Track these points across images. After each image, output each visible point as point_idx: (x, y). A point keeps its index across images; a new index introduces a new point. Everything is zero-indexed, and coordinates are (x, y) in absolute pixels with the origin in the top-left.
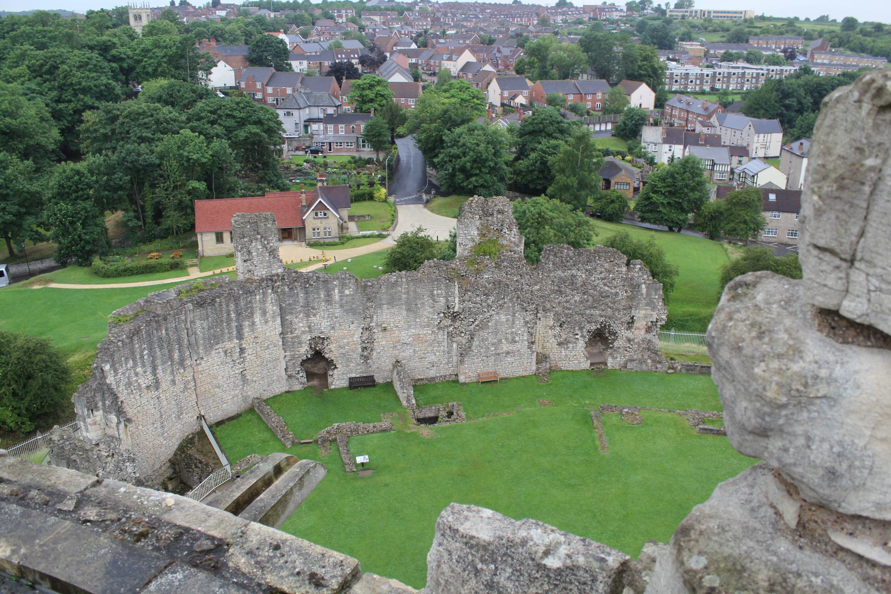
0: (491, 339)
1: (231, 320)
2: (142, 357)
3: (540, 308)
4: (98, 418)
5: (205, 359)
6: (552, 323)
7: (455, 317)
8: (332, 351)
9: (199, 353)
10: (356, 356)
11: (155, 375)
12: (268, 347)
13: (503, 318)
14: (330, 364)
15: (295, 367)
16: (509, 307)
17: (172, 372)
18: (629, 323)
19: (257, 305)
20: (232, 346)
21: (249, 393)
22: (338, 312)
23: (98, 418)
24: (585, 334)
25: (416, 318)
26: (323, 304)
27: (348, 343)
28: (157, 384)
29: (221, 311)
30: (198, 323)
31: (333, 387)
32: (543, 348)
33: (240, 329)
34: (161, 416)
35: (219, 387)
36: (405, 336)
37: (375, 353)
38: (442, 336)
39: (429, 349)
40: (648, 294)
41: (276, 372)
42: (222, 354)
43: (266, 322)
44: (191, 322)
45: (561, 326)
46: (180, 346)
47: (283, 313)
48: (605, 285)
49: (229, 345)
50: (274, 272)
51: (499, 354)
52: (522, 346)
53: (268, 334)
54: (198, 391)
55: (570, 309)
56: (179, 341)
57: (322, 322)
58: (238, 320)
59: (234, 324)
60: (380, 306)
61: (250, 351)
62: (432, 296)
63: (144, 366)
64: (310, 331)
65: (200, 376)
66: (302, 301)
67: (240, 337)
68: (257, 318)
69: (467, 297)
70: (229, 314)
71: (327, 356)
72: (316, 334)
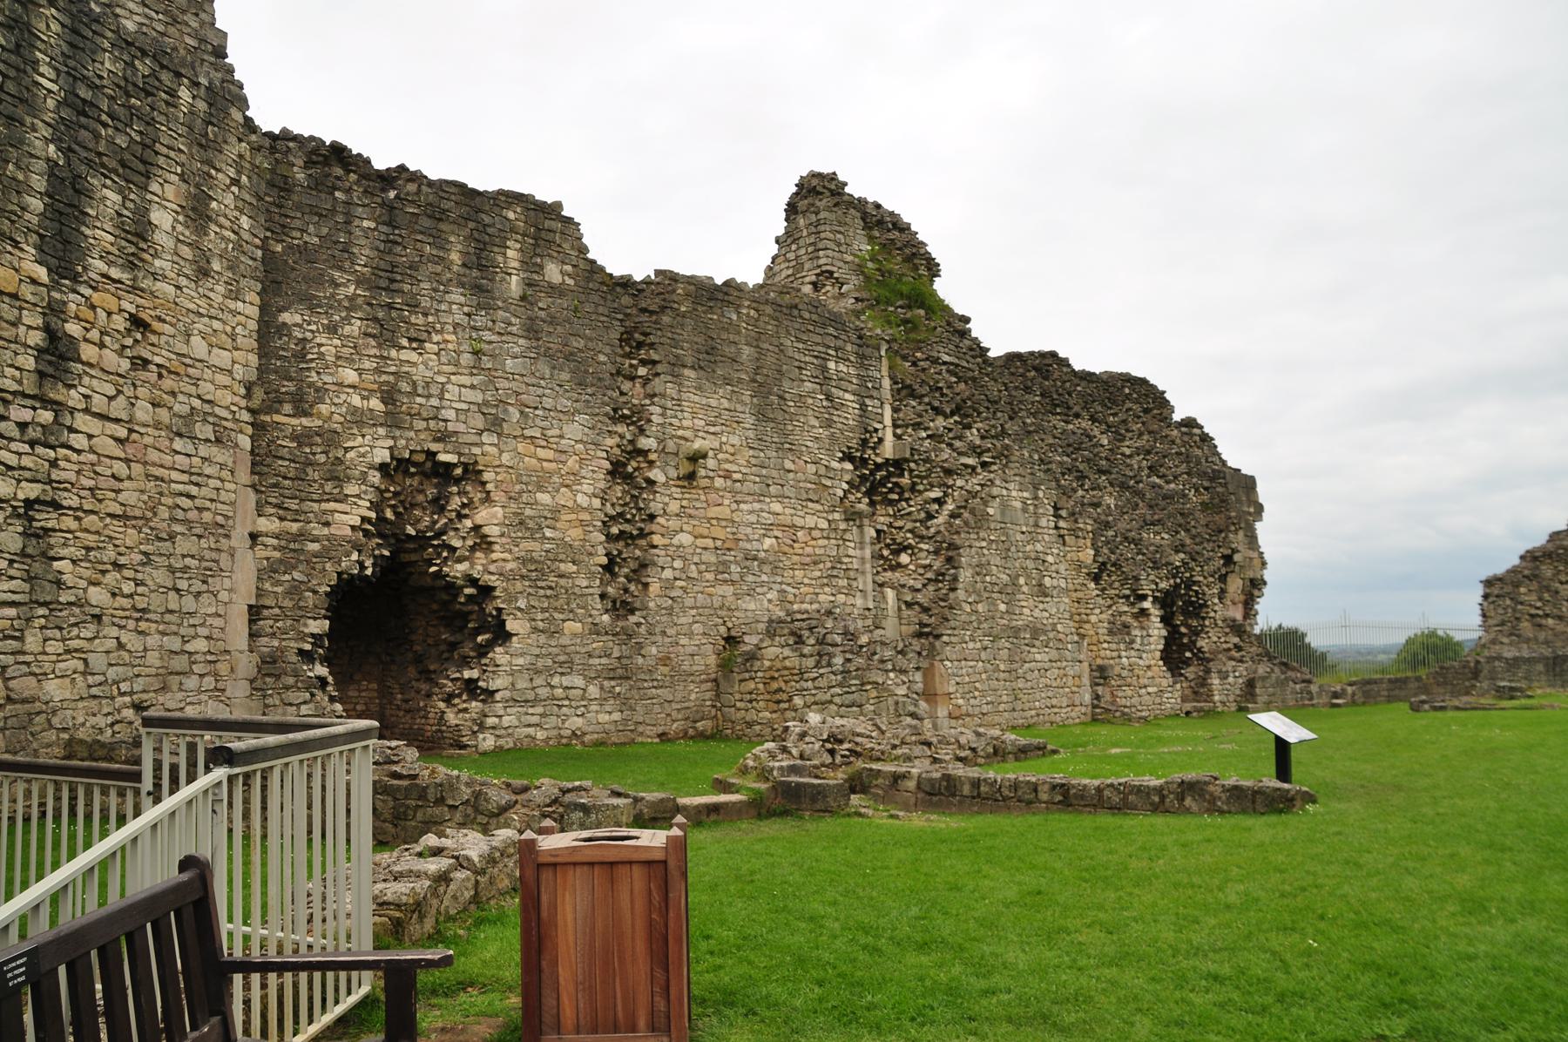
8: (489, 543)
10: (586, 582)
14: (472, 621)
21: (55, 690)
22: (514, 356)
26: (456, 296)
27: (556, 511)
31: (488, 742)
36: (755, 519)
41: (207, 606)
60: (677, 364)
62: (824, 378)
64: (393, 422)
66: (364, 255)
67: (63, 255)
72: (414, 440)
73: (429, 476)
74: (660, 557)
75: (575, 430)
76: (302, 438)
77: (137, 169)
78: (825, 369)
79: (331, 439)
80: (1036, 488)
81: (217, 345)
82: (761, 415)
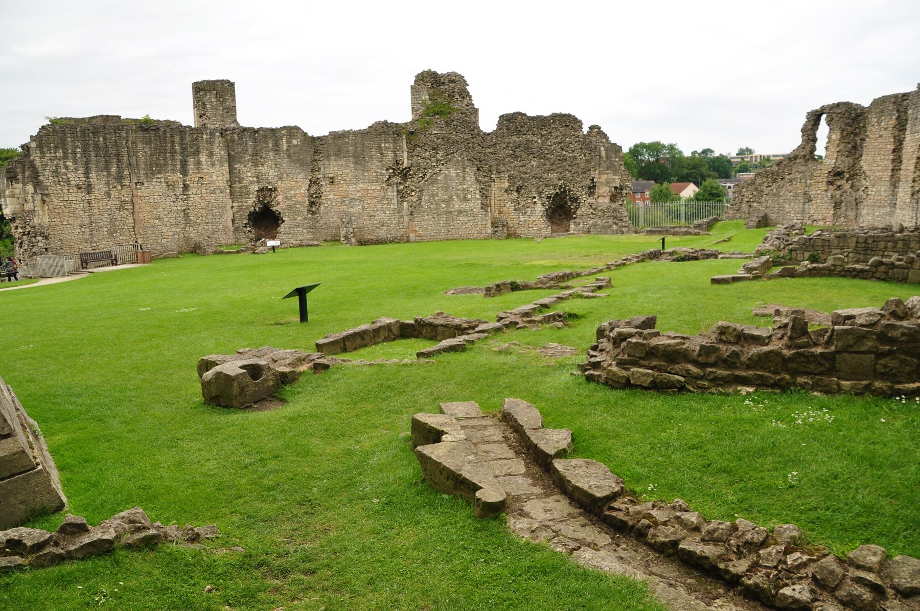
0: (441, 195)
1: (176, 152)
2: (75, 153)
3: (494, 168)
4: (17, 191)
5: (146, 185)
6: (507, 185)
7: (405, 174)
8: (280, 204)
9: (139, 177)
10: (304, 209)
11: (88, 178)
12: (213, 192)
13: (453, 172)
15: (242, 220)
16: (458, 161)
17: (108, 184)
18: (590, 188)
19: (203, 145)
20: (175, 179)
22: (285, 163)
23: (17, 191)
24: (544, 199)
25: (363, 171)
26: (271, 153)
27: (295, 195)
28: (89, 189)
29: (165, 138)
30: (140, 146)
32: (500, 212)
33: (184, 164)
34: (91, 223)
35: (159, 219)
36: (354, 190)
37: (322, 208)
38: (392, 193)
39: (379, 206)
40: (608, 157)
41: (222, 220)
42: (164, 185)
43: (213, 165)
44: (133, 143)
45: (518, 191)
46: (119, 161)
47: (231, 160)
48: (562, 149)
49: (172, 178)
50: (227, 126)
51: (451, 212)
52: (475, 204)
53: (214, 178)
54: (136, 214)
55: (526, 173)
56: (118, 156)
57: (269, 172)
58: (182, 154)
59: (178, 157)
61: (194, 190)
62: (380, 149)
63: (75, 162)
64: (258, 182)
65: (139, 201)
66: (250, 150)
67: (184, 172)
68: (203, 158)
69: (416, 153)
70: (173, 146)
71: (274, 209)
73: (267, 192)
74: (324, 201)
75: (300, 177)
76: (241, 188)
77: (197, 153)
78: (380, 147)
79: (246, 187)
80: (464, 168)
81: (218, 175)
82: (356, 163)
